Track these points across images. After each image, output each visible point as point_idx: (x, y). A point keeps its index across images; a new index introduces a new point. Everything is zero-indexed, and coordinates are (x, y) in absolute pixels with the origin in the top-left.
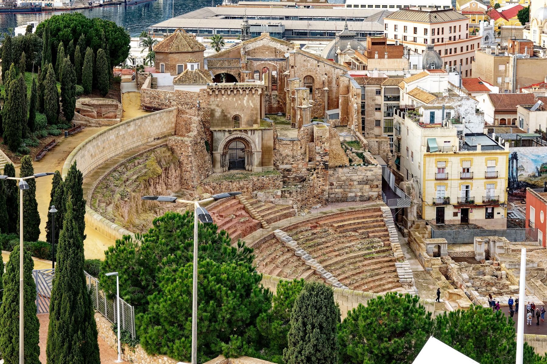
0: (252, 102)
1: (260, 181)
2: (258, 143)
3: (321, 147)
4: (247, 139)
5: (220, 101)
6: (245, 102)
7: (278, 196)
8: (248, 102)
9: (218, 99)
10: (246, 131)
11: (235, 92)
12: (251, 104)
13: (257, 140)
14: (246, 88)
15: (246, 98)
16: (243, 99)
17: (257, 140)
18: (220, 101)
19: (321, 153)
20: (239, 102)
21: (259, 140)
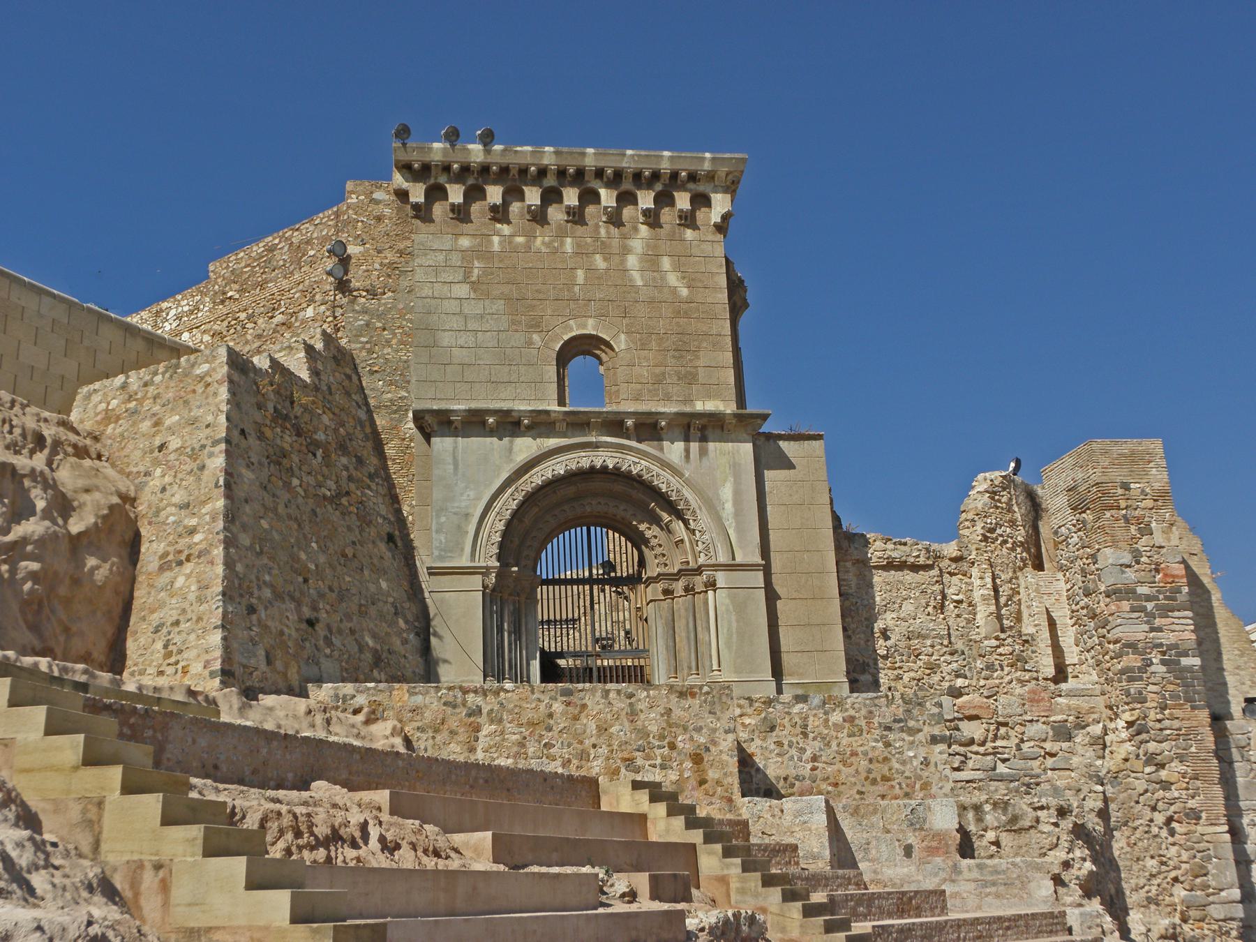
0: (677, 268)
1: (783, 734)
2: (738, 513)
3: (1137, 555)
4: (664, 481)
5: (482, 252)
6: (632, 261)
7: (939, 836)
8: (651, 261)
9: (465, 242)
10: (649, 428)
11: (571, 197)
12: (673, 279)
13: (727, 492)
14: (637, 176)
15: (637, 244)
16: (626, 251)
17: (727, 492)
18: (482, 252)
19: (1143, 590)
20: (600, 263)
21: (737, 494)
